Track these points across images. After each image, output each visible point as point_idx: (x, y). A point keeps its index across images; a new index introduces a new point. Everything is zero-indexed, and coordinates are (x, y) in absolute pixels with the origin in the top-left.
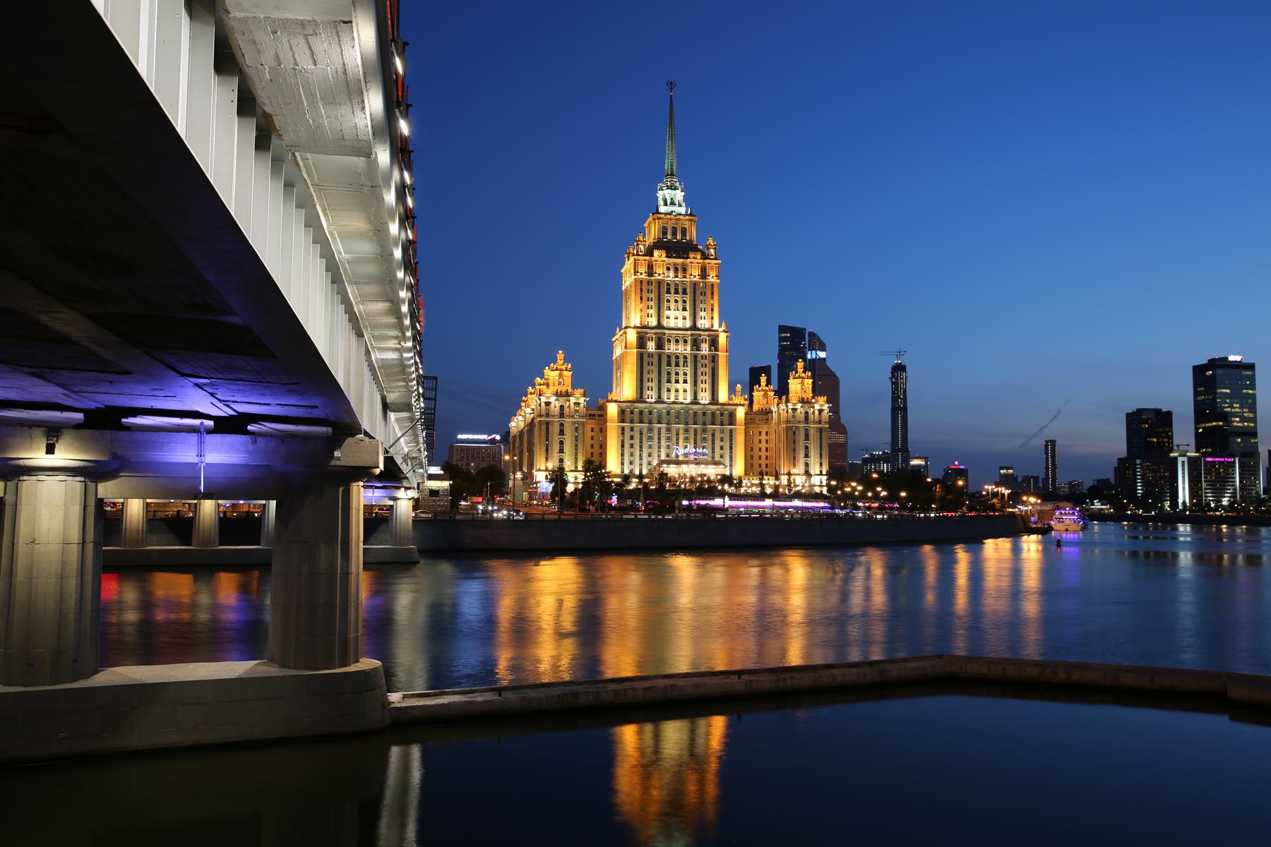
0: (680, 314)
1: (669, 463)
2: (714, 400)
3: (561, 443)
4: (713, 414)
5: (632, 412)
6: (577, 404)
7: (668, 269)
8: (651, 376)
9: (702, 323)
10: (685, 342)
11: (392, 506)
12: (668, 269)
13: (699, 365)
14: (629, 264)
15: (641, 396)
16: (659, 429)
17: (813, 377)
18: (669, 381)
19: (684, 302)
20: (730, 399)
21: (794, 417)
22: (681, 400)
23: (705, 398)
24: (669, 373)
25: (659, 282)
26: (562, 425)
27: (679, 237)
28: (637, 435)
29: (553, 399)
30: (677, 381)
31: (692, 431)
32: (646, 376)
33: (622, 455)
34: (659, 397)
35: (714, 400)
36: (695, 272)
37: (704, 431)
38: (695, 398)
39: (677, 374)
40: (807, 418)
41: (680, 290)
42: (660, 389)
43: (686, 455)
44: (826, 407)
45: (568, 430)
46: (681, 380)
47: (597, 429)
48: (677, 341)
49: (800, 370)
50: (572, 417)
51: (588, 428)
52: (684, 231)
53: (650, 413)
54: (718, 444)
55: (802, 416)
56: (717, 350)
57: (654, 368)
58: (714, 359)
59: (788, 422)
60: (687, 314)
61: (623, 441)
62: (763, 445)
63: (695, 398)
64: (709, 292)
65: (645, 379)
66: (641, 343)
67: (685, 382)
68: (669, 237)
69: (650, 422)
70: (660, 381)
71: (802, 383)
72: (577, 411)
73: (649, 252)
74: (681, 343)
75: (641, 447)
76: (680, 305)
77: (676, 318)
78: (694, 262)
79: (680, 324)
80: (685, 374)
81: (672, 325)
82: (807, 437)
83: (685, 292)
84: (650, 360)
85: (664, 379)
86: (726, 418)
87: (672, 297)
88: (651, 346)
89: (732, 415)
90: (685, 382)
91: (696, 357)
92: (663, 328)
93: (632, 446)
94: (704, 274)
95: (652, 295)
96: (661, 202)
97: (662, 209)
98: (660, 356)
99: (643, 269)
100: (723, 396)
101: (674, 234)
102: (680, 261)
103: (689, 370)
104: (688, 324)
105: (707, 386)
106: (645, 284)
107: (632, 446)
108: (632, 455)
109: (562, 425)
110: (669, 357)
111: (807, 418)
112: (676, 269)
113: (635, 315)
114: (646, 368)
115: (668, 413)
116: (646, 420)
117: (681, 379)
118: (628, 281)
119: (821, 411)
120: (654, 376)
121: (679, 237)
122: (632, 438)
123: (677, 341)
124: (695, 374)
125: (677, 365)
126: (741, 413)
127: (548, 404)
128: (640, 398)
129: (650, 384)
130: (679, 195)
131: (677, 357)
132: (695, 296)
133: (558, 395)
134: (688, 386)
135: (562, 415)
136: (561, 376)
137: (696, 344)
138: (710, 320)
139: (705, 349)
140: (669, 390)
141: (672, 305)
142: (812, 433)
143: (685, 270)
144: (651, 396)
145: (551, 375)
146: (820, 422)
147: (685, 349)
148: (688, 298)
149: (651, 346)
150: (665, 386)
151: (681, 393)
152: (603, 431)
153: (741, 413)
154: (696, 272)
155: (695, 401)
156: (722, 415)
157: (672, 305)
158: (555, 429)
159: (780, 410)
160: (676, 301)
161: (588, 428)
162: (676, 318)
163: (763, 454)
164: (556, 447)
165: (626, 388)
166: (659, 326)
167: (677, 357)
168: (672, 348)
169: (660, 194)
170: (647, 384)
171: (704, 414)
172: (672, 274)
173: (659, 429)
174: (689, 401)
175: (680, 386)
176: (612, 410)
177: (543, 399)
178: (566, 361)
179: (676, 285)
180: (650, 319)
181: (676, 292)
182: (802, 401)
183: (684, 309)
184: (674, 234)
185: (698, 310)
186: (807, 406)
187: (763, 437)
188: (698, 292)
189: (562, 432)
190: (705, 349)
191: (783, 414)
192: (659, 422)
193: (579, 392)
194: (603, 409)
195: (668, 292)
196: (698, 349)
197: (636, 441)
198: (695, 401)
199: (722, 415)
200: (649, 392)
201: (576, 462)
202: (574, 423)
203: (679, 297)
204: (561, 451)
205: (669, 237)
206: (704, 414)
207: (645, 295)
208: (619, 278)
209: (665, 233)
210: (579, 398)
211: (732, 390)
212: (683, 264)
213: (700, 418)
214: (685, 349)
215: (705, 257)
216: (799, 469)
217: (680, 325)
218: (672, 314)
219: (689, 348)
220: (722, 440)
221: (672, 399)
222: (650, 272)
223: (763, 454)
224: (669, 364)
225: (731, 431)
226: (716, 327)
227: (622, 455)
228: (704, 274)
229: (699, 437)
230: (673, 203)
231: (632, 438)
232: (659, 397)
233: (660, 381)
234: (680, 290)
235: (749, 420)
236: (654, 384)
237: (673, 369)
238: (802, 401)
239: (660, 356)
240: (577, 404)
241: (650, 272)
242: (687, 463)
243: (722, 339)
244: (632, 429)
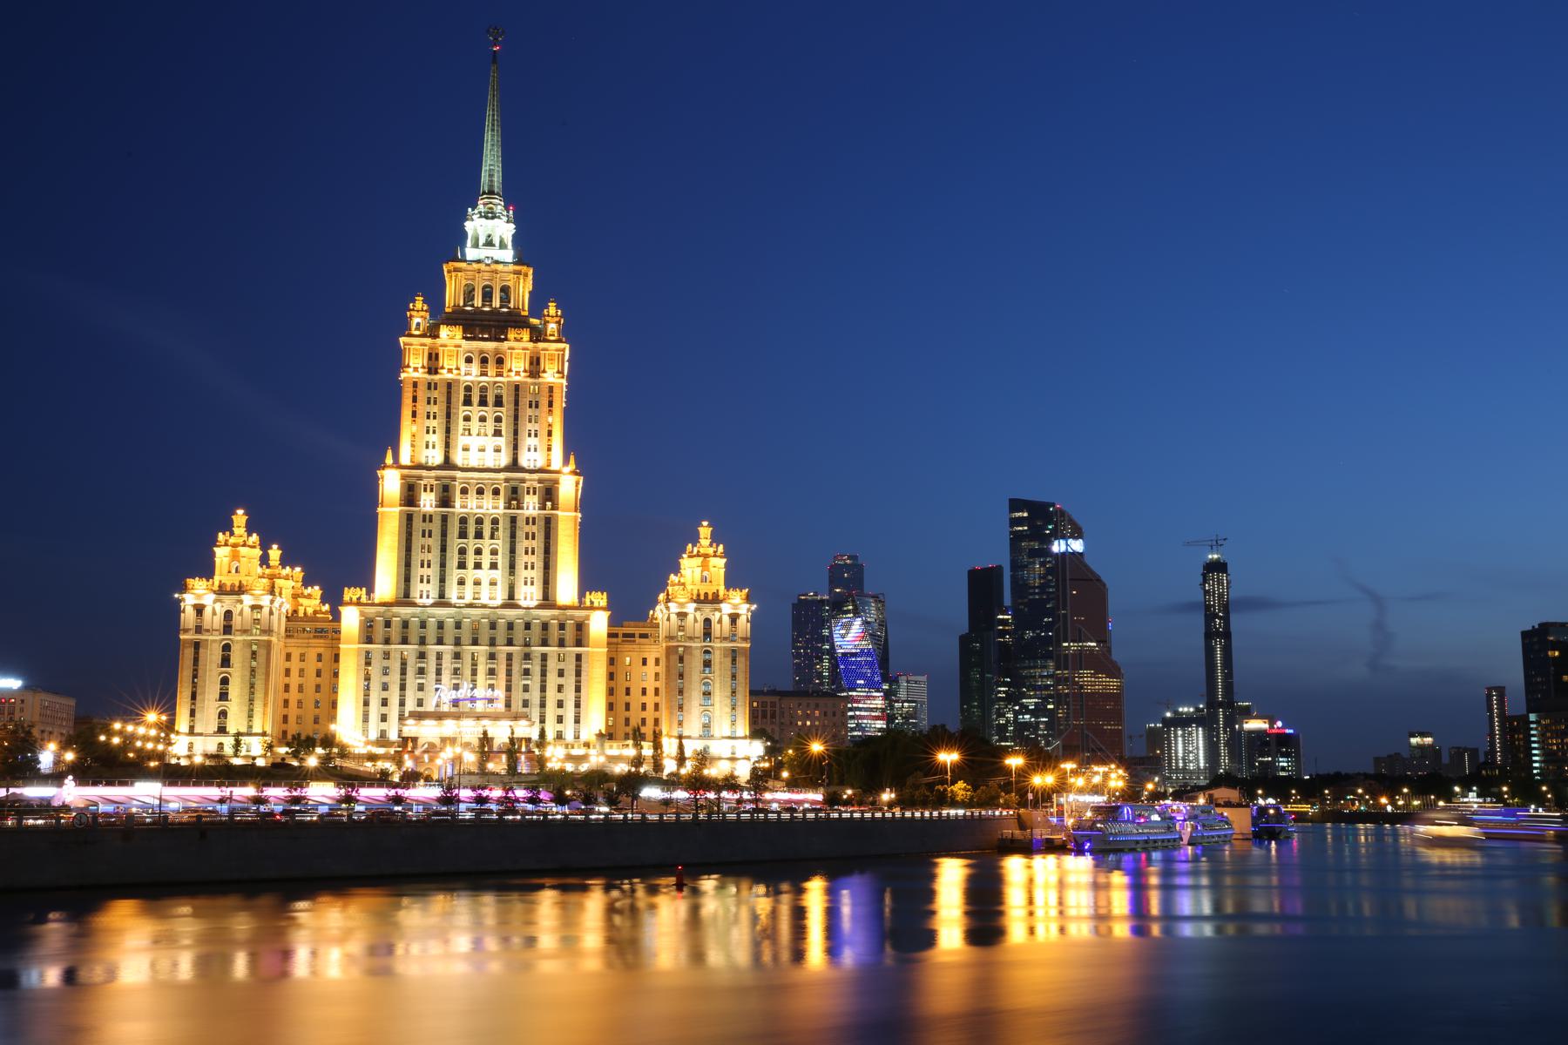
1: (419, 716)
2: (547, 601)
3: (225, 681)
5: (388, 624)
6: (256, 608)
7: (469, 360)
8: (427, 557)
10: (496, 492)
12: (469, 360)
13: (520, 534)
15: (407, 595)
16: (439, 656)
17: (726, 554)
18: (462, 566)
19: (498, 420)
20: (581, 595)
21: (681, 628)
22: (484, 600)
23: (529, 595)
24: (462, 552)
26: (227, 648)
27: (496, 303)
28: (396, 666)
29: (208, 600)
30: (478, 566)
31: (502, 658)
32: (417, 557)
33: (366, 704)
34: (442, 595)
35: (547, 601)
36: (517, 367)
37: (527, 657)
38: (511, 596)
39: (478, 552)
40: (707, 634)
41: (491, 399)
42: (442, 580)
43: (455, 703)
44: (745, 610)
45: (236, 656)
47: (327, 656)
48: (480, 492)
49: (705, 542)
50: (245, 632)
52: (505, 290)
53: (423, 625)
54: (553, 680)
55: (700, 626)
56: (555, 507)
57: (434, 542)
58: (549, 525)
59: (670, 638)
61: (368, 678)
63: (511, 596)
64: (544, 402)
65: (416, 562)
66: (410, 497)
67: (494, 566)
68: (478, 302)
69: (458, 642)
70: (443, 565)
71: (705, 566)
72: (257, 621)
73: (433, 332)
74: (488, 494)
75: (403, 688)
76: (490, 426)
78: (517, 347)
79: (490, 460)
80: (494, 552)
81: (474, 460)
82: (707, 664)
83: (499, 402)
84: (427, 526)
85: (453, 559)
86: (569, 634)
87: (475, 411)
88: (427, 502)
89: (580, 627)
90: (494, 566)
91: (513, 520)
92: (455, 468)
93: (385, 687)
95: (434, 409)
96: (469, 243)
98: (444, 518)
101: (488, 295)
102: (490, 345)
103: (501, 544)
104: (504, 459)
105: (536, 574)
106: (422, 389)
107: (385, 687)
108: (385, 703)
109: (227, 648)
110: (463, 521)
112: (484, 361)
114: (418, 541)
115: (458, 625)
116: (414, 637)
117: (486, 559)
119: (734, 618)
120: (434, 557)
121: (496, 303)
122: (385, 672)
123: (480, 492)
124: (513, 551)
125: (479, 535)
128: (405, 599)
129: (425, 571)
130: (504, 229)
131: (479, 521)
132: (513, 407)
134: (498, 575)
135: (227, 629)
136: (235, 557)
137: (514, 497)
138: (546, 450)
139: (531, 505)
140: (461, 582)
141: (475, 425)
142: (716, 658)
143: (500, 361)
144: (424, 592)
146: (732, 637)
147: (492, 507)
148: (504, 412)
149: (427, 502)
150: (454, 574)
151: (482, 587)
155: (511, 602)
156: (562, 627)
158: (212, 656)
160: (483, 419)
161: (312, 655)
162: (480, 447)
164: (211, 690)
165: (386, 581)
166: (448, 464)
167: (479, 521)
169: (469, 226)
170: (417, 572)
171: (528, 626)
172: (475, 368)
173: (439, 656)
174: (499, 602)
175: (485, 574)
176: (351, 619)
179: (483, 389)
180: (430, 452)
181: (483, 402)
182: (702, 600)
183: (497, 433)
184: (488, 295)
185: (523, 434)
186: (707, 608)
188: (524, 402)
189: (226, 662)
190: (531, 505)
192: (440, 642)
195: (468, 402)
196: (519, 507)
197: (394, 679)
198: (511, 602)
199: (562, 627)
200: (424, 587)
201: (250, 716)
202: (250, 644)
203: (490, 411)
204: (224, 696)
205: (478, 302)
206: (528, 626)
207: (422, 408)
209: (469, 294)
211: (587, 583)
212: (497, 351)
213: (519, 634)
214: (492, 507)
215: (538, 335)
217: (490, 464)
218: (474, 442)
219: (501, 502)
220: (561, 673)
221: (468, 599)
222: (433, 370)
224: (463, 535)
225: (579, 657)
227: (366, 704)
229: (516, 669)
230: (489, 243)
231: (385, 672)
232: (442, 595)
233: (443, 565)
234: (491, 399)
236: (433, 572)
237: (471, 544)
239: (444, 518)
240: (256, 608)
241: (433, 370)
242: (457, 717)
244: (387, 655)
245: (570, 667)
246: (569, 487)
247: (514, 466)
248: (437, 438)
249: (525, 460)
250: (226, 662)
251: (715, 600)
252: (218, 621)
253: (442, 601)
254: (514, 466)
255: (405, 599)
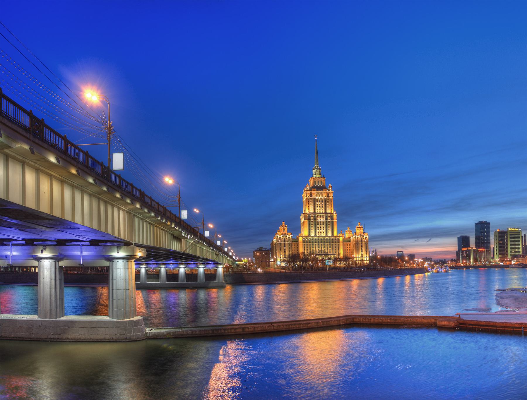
0: (321, 208)
2: (333, 235)
4: (333, 239)
6: (289, 237)
9: (328, 211)
11: (108, 268)
14: (304, 194)
23: (330, 234)
25: (314, 199)
28: (309, 246)
35: (333, 235)
45: (286, 245)
46: (322, 228)
47: (296, 245)
51: (293, 245)
52: (321, 182)
58: (332, 223)
60: (323, 208)
62: (349, 249)
77: (320, 210)
88: (312, 219)
89: (338, 239)
94: (328, 196)
97: (314, 176)
99: (309, 195)
100: (335, 233)
111: (362, 241)
113: (307, 210)
117: (322, 228)
118: (304, 199)
126: (341, 239)
127: (280, 238)
128: (309, 235)
133: (283, 235)
134: (324, 231)
136: (284, 229)
138: (331, 210)
139: (329, 219)
144: (312, 234)
145: (281, 229)
149: (312, 219)
152: (298, 245)
153: (341, 239)
154: (326, 195)
155: (327, 236)
157: (319, 206)
159: (354, 238)
162: (320, 210)
163: (349, 251)
166: (315, 212)
168: (318, 219)
175: (322, 231)
176: (301, 239)
177: (279, 236)
178: (285, 224)
187: (349, 246)
189: (285, 246)
190: (329, 219)
191: (354, 239)
193: (289, 234)
194: (298, 239)
198: (327, 236)
203: (320, 203)
208: (302, 198)
210: (290, 236)
216: (360, 256)
218: (319, 208)
223: (349, 251)
226: (333, 212)
228: (328, 196)
235: (344, 241)
237: (320, 226)
238: (360, 235)
240: (289, 237)
241: (311, 196)
243: (335, 216)
245: (337, 246)
246: (335, 216)
247: (326, 212)
248: (312, 208)
249: (328, 211)
250: (285, 246)
251: (363, 235)
252: (283, 239)
253: (315, 236)
254: (326, 212)
255: (309, 235)
